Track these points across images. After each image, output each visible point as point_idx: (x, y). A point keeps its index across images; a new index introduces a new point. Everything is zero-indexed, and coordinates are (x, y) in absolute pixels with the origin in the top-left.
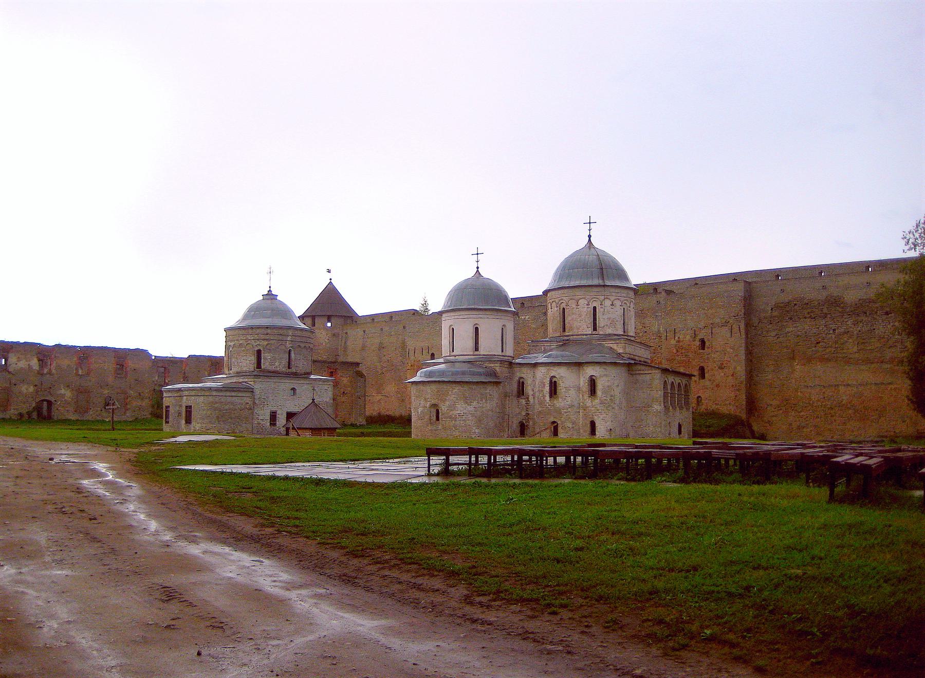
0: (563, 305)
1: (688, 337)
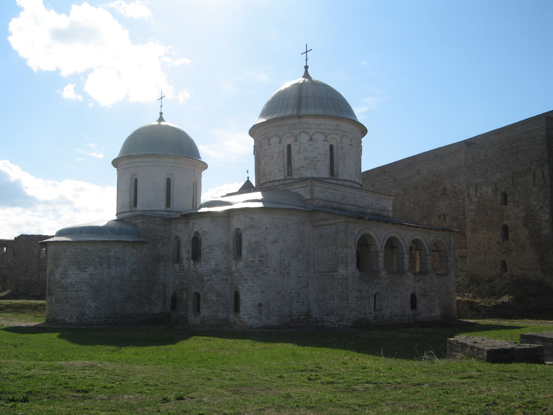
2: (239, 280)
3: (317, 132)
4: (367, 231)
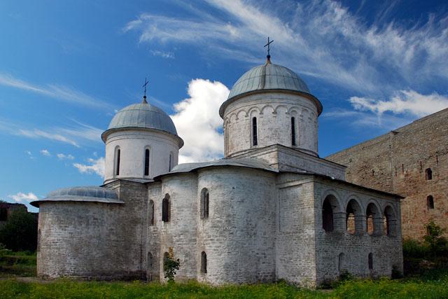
1: (415, 170)
2: (206, 240)
3: (280, 106)
4: (331, 193)
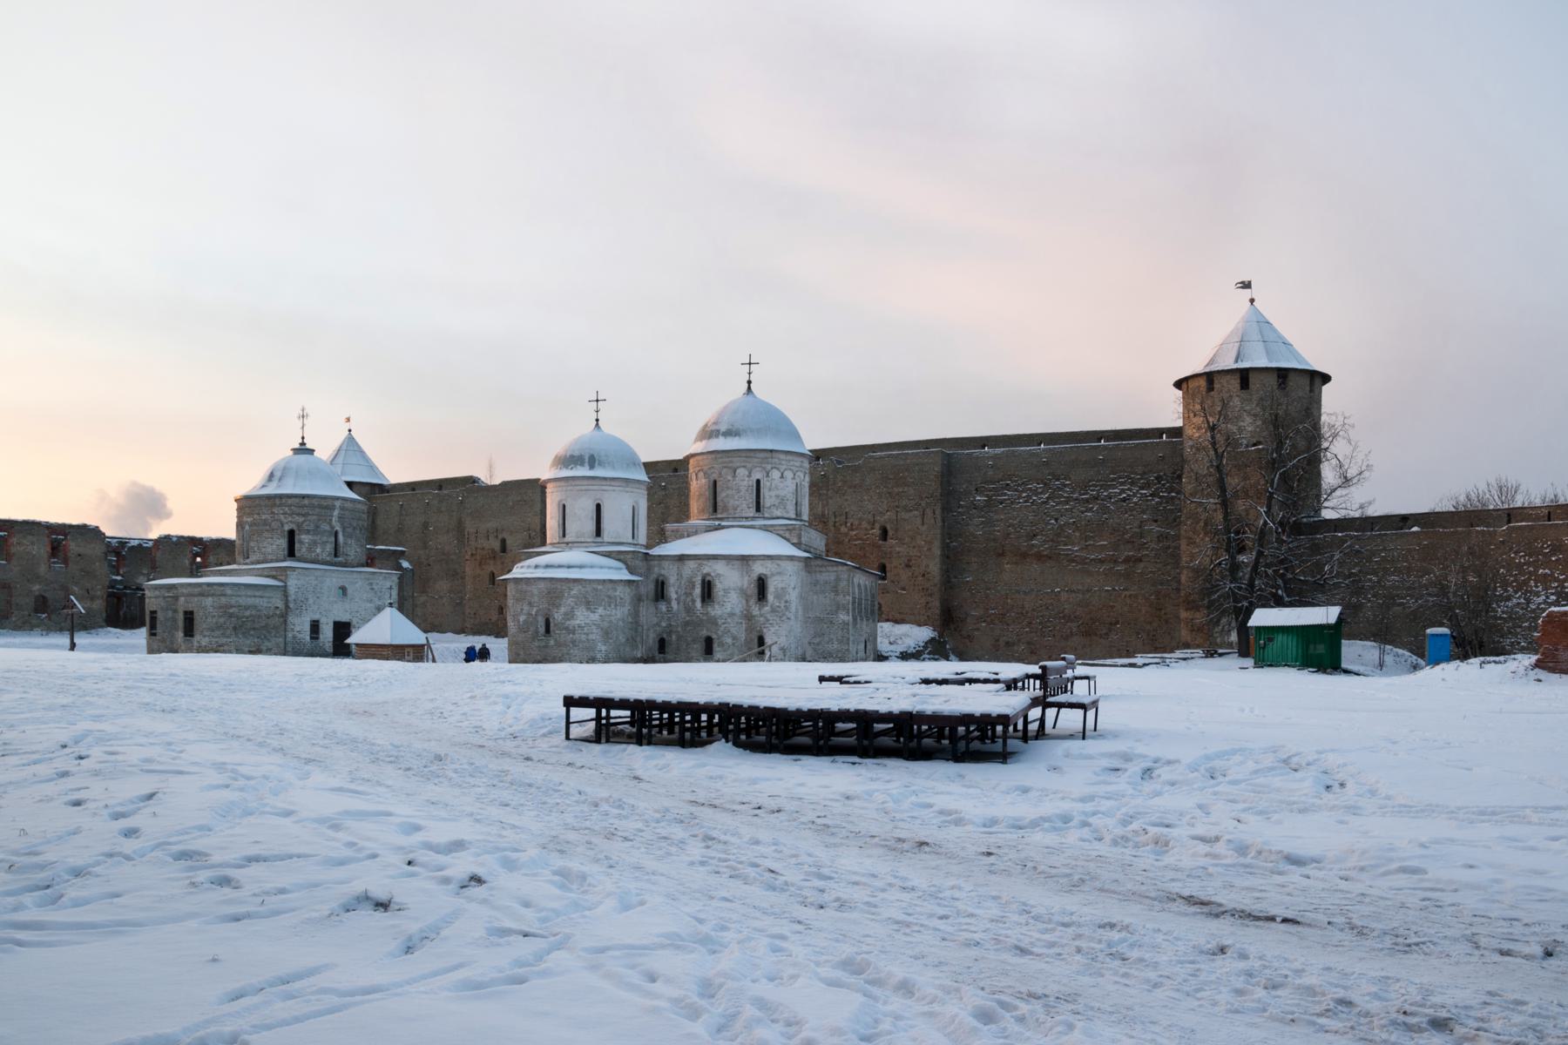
0: (715, 476)
